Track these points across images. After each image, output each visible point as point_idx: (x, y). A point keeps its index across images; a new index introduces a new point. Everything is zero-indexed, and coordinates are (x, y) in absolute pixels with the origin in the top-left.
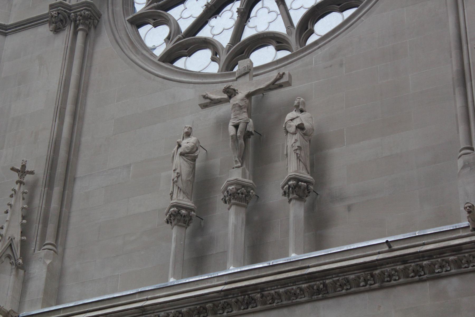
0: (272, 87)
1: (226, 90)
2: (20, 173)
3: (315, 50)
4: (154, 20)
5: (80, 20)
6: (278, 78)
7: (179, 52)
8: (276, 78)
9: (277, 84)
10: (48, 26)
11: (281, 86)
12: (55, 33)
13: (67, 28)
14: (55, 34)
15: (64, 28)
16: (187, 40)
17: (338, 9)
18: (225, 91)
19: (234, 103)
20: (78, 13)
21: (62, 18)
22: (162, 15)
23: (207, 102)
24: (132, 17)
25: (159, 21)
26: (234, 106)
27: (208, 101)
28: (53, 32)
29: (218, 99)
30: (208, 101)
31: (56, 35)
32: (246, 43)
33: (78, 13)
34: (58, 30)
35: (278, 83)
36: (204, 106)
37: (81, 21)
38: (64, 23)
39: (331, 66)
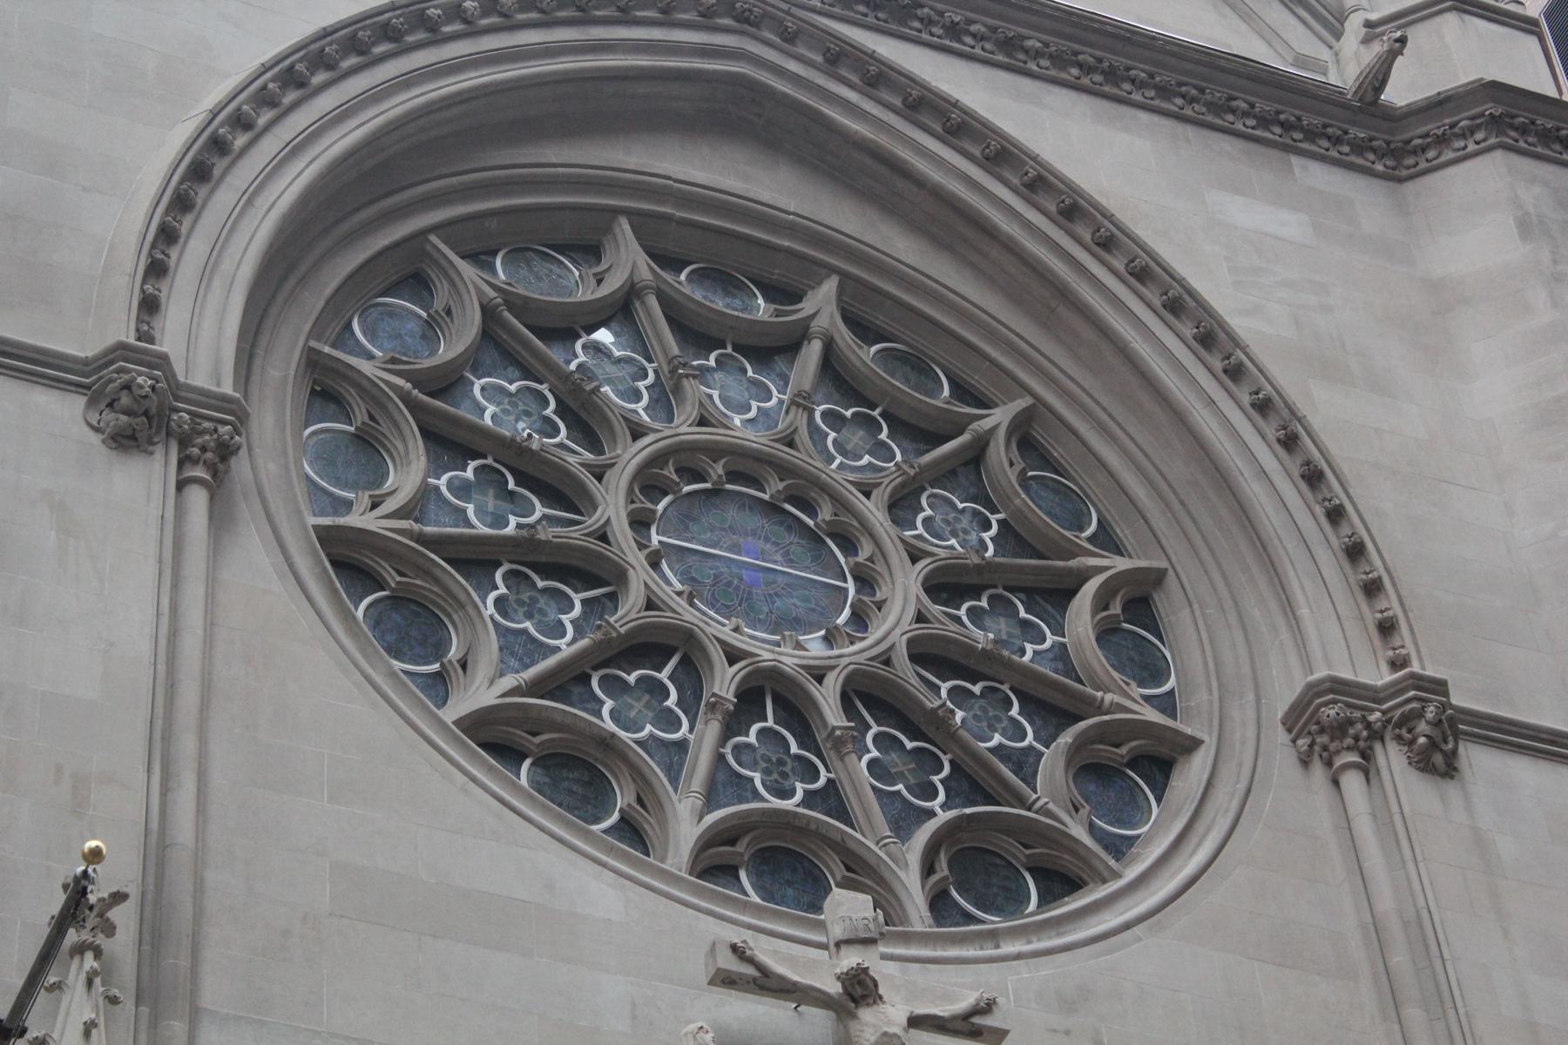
0: (959, 1025)
1: (859, 975)
2: (92, 916)
3: (604, 865)
4: (952, 712)
5: (204, 449)
6: (983, 1008)
7: (511, 730)
8: (978, 1004)
9: (973, 1024)
10: (82, 406)
11: (975, 1033)
12: (114, 445)
13: (159, 450)
14: (111, 448)
15: (151, 448)
16: (547, 707)
17: (1024, 860)
18: (855, 976)
19: (886, 1029)
20: (207, 425)
21: (154, 411)
22: (438, 573)
23: (743, 974)
24: (331, 523)
25: (417, 586)
26: (885, 1039)
27: (750, 971)
28: (101, 437)
29: (782, 978)
30: (750, 971)
31: (114, 452)
32: (752, 819)
33: (207, 425)
34: (119, 438)
35: (977, 1020)
36: (726, 980)
37: (209, 455)
38: (154, 430)
39: (1067, 1033)
